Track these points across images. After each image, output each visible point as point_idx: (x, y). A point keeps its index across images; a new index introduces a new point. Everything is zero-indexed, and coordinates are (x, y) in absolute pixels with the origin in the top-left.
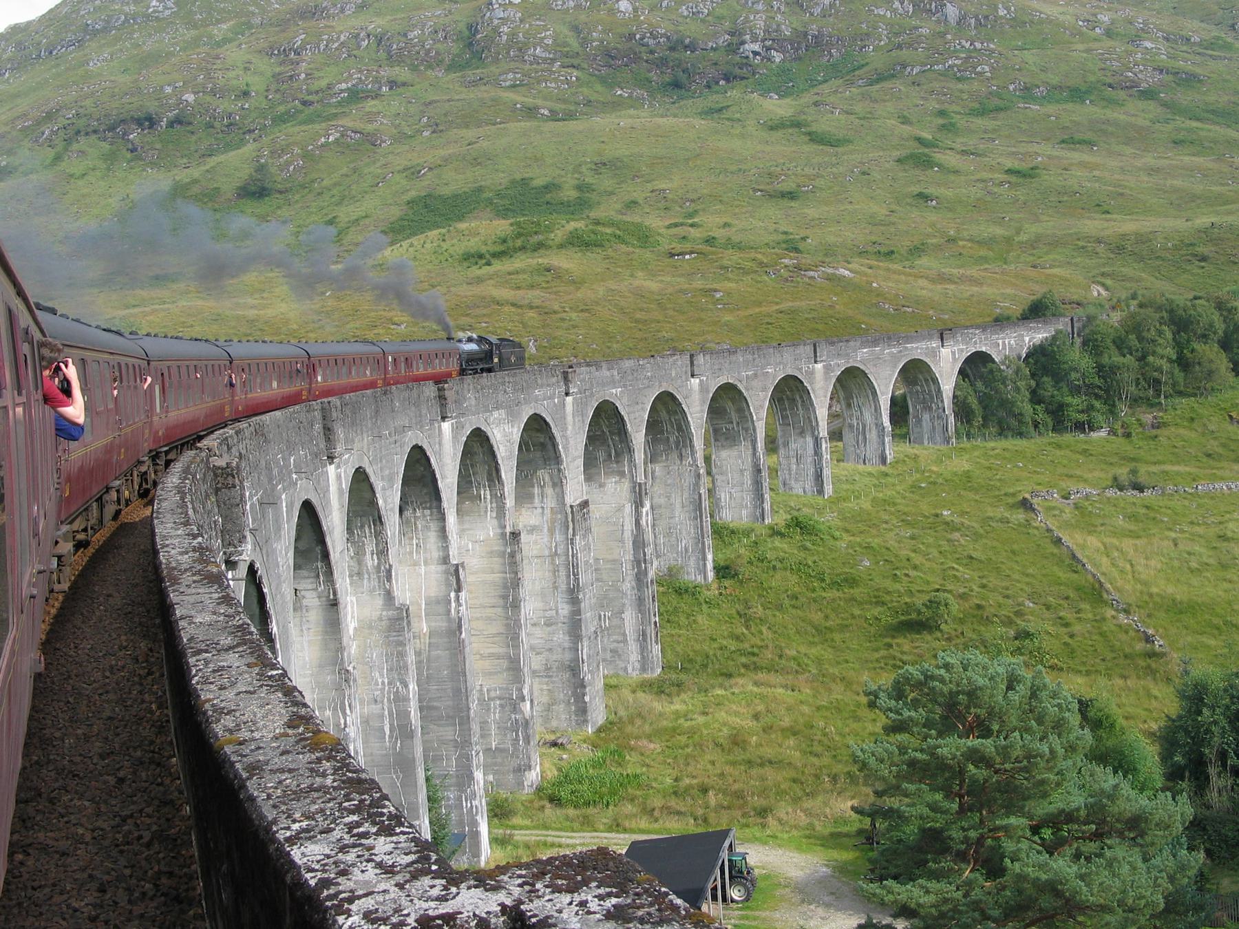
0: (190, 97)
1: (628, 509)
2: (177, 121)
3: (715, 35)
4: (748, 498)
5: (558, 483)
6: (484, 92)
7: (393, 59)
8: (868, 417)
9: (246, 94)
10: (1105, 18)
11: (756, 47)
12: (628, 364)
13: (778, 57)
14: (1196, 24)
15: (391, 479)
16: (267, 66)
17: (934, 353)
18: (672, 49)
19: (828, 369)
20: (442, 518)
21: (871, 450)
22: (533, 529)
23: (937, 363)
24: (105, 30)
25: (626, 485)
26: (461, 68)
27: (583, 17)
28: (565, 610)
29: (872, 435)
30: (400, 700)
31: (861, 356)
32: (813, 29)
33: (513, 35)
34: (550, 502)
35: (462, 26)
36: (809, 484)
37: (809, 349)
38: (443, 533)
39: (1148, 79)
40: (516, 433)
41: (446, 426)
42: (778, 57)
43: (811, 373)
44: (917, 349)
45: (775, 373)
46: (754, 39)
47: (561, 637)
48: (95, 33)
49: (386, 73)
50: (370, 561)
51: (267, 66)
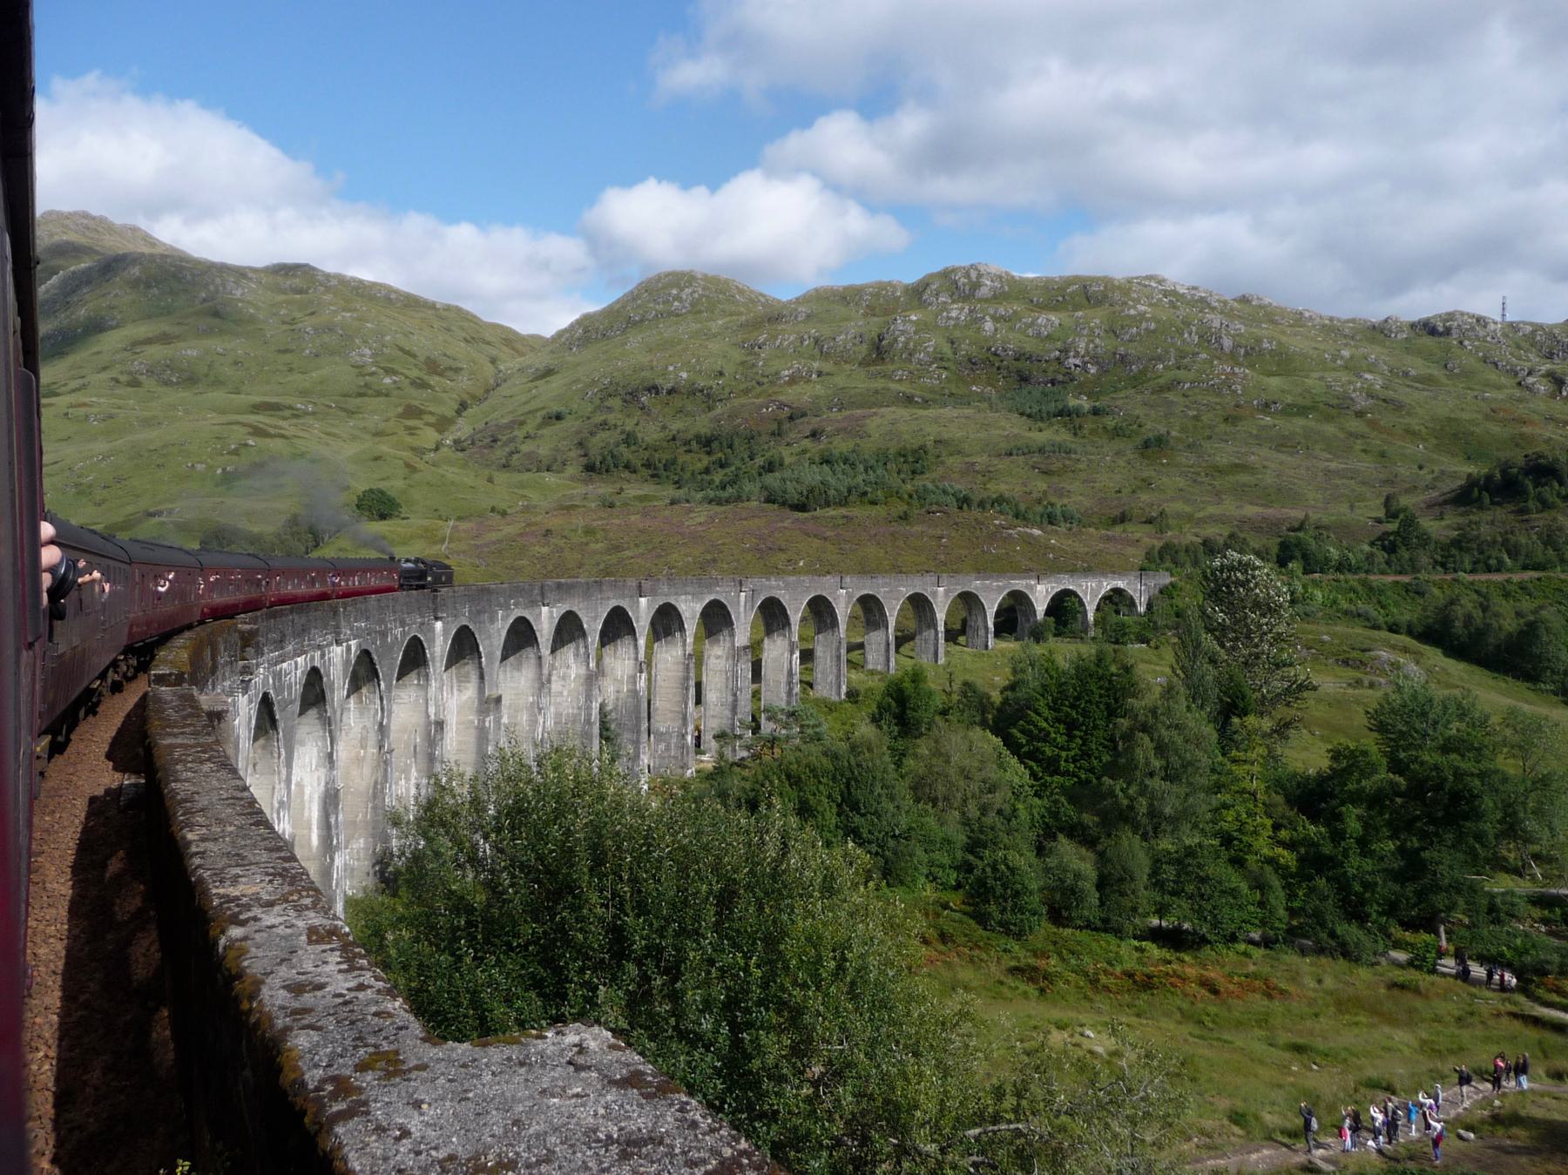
0: (684, 375)
1: (786, 655)
2: (670, 392)
3: (1050, 351)
4: (882, 659)
5: (732, 635)
6: (879, 384)
7: (825, 356)
8: (980, 622)
9: (721, 374)
10: (1346, 353)
11: (1077, 362)
12: (792, 579)
13: (1093, 370)
14: (1419, 362)
15: (595, 618)
16: (738, 355)
17: (1032, 588)
18: (1017, 360)
19: (947, 592)
20: (636, 640)
21: (980, 642)
22: (718, 657)
23: (1034, 593)
24: (642, 321)
25: (787, 642)
26: (868, 365)
27: (957, 334)
28: (730, 699)
29: (982, 632)
30: (589, 708)
31: (975, 585)
32: (1122, 350)
33: (906, 344)
34: (728, 645)
35: (874, 335)
36: (931, 656)
37: (934, 579)
38: (636, 646)
39: (1362, 402)
40: (699, 607)
41: (643, 600)
42: (1093, 370)
43: (935, 594)
44: (1019, 584)
45: (906, 591)
46: (1077, 355)
47: (728, 713)
48: (635, 324)
49: (816, 365)
50: (582, 650)
51: (738, 355)
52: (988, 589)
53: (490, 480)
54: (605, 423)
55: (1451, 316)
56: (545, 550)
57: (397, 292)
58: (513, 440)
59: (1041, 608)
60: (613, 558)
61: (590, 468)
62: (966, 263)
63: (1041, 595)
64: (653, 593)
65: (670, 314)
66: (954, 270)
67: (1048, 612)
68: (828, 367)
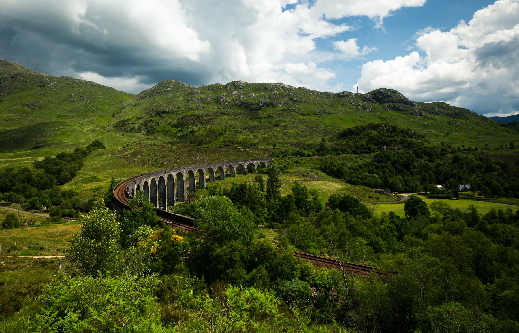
44: (241, 163)
45: (217, 166)
52: (234, 164)
53: (123, 135)
54: (151, 120)
55: (343, 92)
56: (140, 156)
57: (95, 83)
58: (128, 124)
59: (246, 167)
60: (156, 158)
61: (148, 132)
62: (237, 80)
63: (246, 165)
64: (168, 172)
65: (166, 91)
66: (235, 82)
67: (247, 168)
68: (205, 106)
